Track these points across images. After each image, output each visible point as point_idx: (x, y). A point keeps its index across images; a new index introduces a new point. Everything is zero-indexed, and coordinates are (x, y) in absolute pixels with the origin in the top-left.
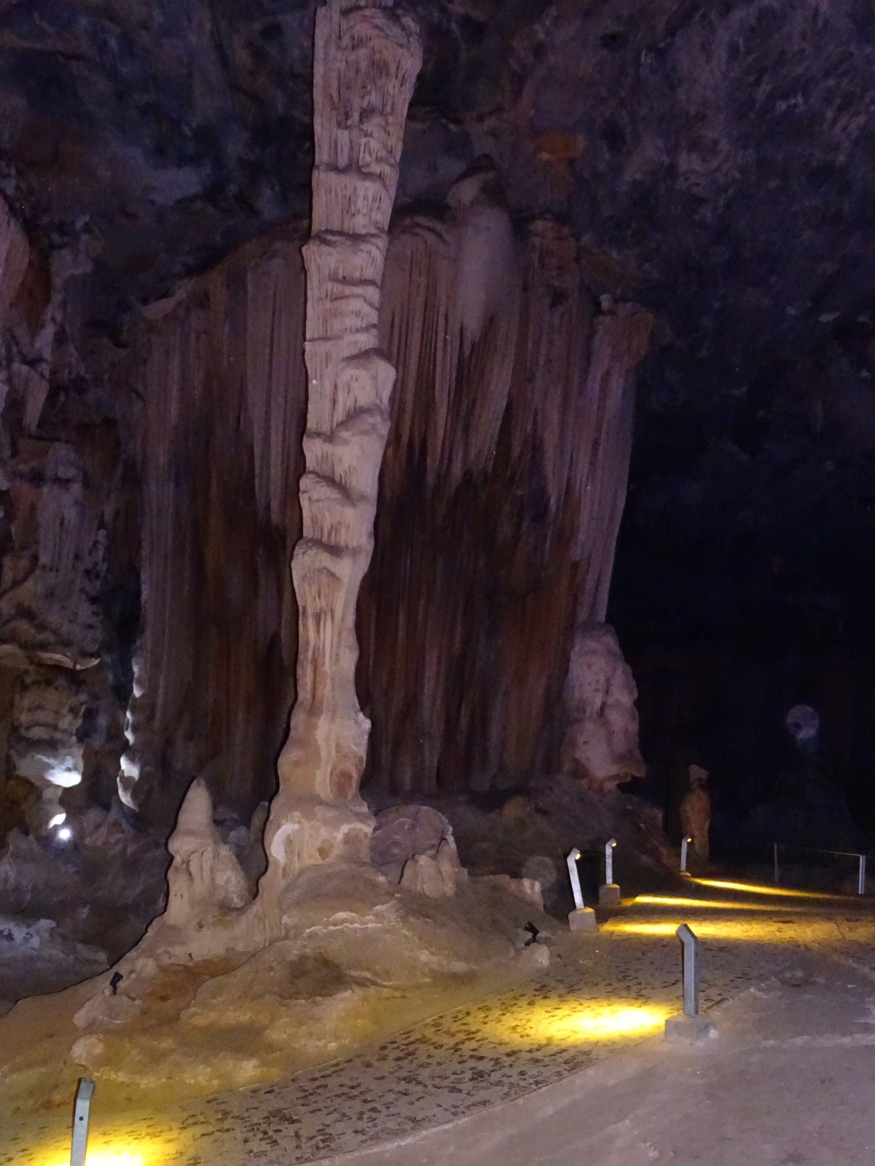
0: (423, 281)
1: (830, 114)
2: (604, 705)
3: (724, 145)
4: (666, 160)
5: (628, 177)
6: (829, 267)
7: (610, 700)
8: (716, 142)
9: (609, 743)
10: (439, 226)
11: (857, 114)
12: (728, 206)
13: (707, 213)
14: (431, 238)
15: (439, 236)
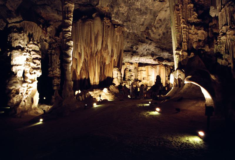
0: (90, 27)
1: (136, 2)
2: (117, 76)
3: (124, 7)
4: (118, 9)
5: (114, 11)
6: (143, 20)
7: (118, 76)
8: (123, 7)
9: (118, 81)
10: (92, 20)
11: (139, 2)
12: (127, 14)
13: (125, 15)
14: (90, 21)
15: (91, 21)
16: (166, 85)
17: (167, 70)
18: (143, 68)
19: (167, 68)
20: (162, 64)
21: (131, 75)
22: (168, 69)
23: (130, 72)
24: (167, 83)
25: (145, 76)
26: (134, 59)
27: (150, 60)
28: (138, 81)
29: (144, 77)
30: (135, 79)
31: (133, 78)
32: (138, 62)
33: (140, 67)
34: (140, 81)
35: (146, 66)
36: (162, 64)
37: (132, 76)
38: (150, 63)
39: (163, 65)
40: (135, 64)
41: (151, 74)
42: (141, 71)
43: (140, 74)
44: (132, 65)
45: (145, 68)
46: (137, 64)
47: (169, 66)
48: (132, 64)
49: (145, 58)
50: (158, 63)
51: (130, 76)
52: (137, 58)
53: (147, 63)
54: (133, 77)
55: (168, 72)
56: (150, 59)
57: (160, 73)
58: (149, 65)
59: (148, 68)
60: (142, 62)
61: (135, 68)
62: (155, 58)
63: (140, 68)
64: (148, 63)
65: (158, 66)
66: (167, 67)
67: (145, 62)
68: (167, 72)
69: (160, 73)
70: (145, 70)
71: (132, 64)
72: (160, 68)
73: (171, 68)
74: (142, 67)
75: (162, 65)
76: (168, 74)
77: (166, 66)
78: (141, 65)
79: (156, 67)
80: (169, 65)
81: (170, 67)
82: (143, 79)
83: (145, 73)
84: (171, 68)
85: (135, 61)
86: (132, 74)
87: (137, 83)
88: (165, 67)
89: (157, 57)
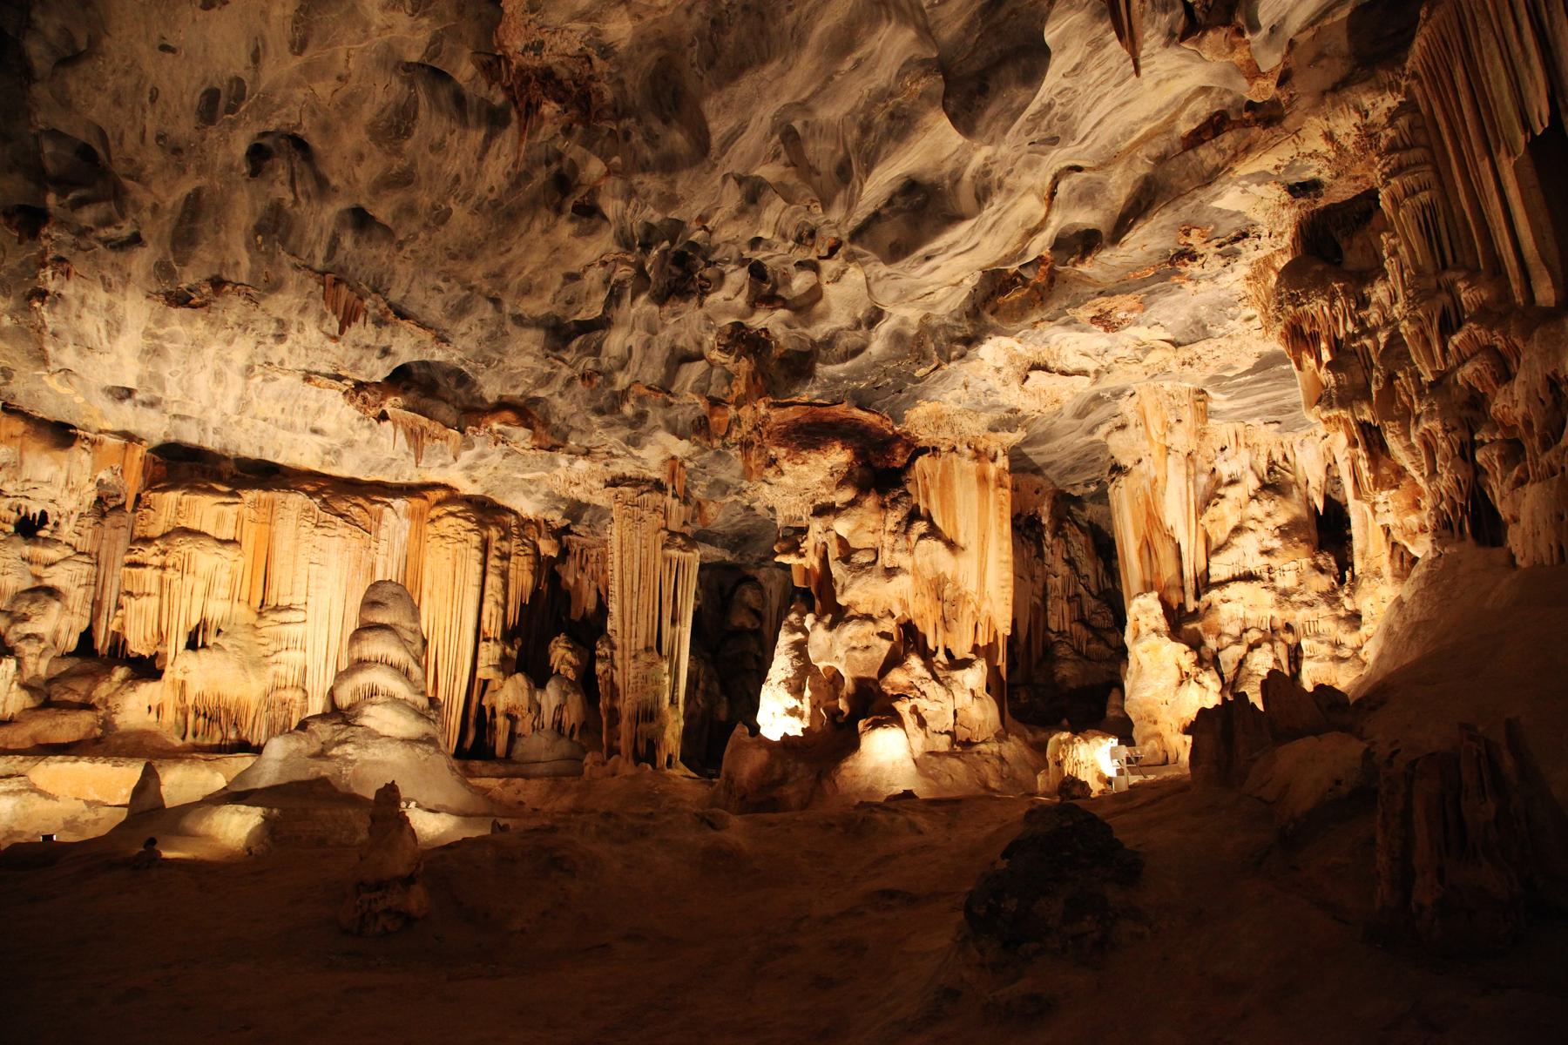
16: (471, 736)
17: (493, 562)
18: (205, 510)
19: (494, 544)
20: (441, 494)
21: (28, 583)
22: (505, 557)
23: (27, 550)
24: (481, 708)
25: (217, 610)
26: (83, 345)
27: (311, 391)
28: (120, 673)
29: (203, 626)
30: (87, 637)
31: (58, 625)
32: (155, 427)
33: (172, 496)
34: (147, 669)
35: (250, 496)
36: (441, 494)
37: (53, 593)
38: (303, 453)
39: (452, 496)
40: (111, 441)
41: (300, 588)
42: (165, 536)
43: (150, 576)
44: (63, 455)
45: (230, 511)
46: (140, 452)
47: (525, 523)
48: (62, 434)
49: (241, 352)
50: (410, 474)
51: (18, 596)
52: (115, 327)
53: (269, 457)
54: (57, 605)
55: (506, 586)
56: (308, 377)
57: (412, 562)
58: (297, 490)
59: (270, 515)
60: (211, 443)
61: (105, 506)
62: (379, 370)
63: (170, 505)
64: (286, 457)
65: (399, 503)
66: (494, 533)
67: (248, 443)
68: (493, 580)
69: (412, 562)
70: (227, 533)
71: (62, 434)
72: (419, 535)
73: (547, 548)
74: (193, 488)
75: (439, 503)
76: (505, 607)
77: (485, 510)
78: (183, 465)
79: (379, 519)
80: (527, 507)
81: (532, 532)
82: (192, 645)
83: (223, 576)
84: (547, 548)
85: (104, 404)
86: (57, 577)
87: (103, 689)
88: (482, 524)
89: (408, 347)
